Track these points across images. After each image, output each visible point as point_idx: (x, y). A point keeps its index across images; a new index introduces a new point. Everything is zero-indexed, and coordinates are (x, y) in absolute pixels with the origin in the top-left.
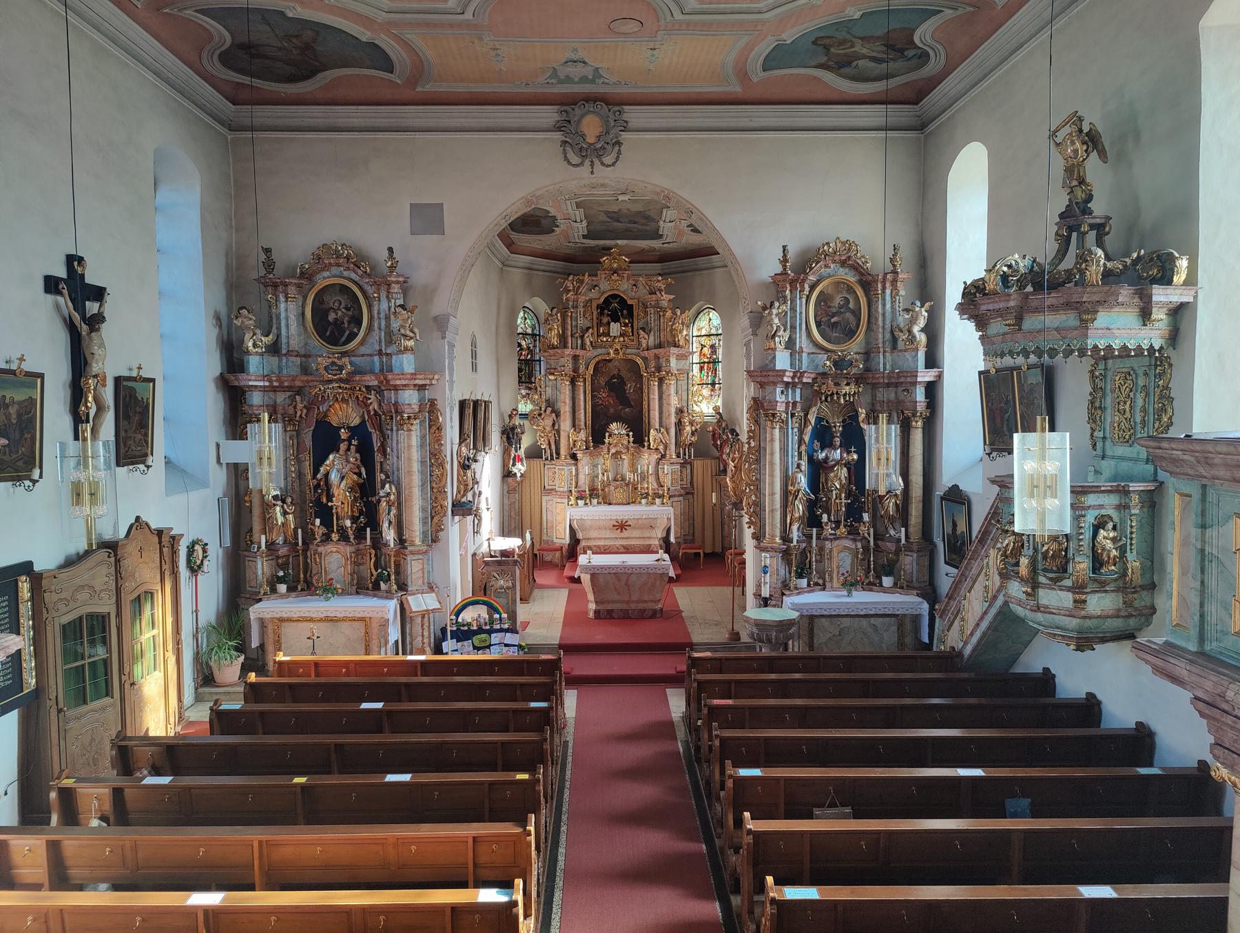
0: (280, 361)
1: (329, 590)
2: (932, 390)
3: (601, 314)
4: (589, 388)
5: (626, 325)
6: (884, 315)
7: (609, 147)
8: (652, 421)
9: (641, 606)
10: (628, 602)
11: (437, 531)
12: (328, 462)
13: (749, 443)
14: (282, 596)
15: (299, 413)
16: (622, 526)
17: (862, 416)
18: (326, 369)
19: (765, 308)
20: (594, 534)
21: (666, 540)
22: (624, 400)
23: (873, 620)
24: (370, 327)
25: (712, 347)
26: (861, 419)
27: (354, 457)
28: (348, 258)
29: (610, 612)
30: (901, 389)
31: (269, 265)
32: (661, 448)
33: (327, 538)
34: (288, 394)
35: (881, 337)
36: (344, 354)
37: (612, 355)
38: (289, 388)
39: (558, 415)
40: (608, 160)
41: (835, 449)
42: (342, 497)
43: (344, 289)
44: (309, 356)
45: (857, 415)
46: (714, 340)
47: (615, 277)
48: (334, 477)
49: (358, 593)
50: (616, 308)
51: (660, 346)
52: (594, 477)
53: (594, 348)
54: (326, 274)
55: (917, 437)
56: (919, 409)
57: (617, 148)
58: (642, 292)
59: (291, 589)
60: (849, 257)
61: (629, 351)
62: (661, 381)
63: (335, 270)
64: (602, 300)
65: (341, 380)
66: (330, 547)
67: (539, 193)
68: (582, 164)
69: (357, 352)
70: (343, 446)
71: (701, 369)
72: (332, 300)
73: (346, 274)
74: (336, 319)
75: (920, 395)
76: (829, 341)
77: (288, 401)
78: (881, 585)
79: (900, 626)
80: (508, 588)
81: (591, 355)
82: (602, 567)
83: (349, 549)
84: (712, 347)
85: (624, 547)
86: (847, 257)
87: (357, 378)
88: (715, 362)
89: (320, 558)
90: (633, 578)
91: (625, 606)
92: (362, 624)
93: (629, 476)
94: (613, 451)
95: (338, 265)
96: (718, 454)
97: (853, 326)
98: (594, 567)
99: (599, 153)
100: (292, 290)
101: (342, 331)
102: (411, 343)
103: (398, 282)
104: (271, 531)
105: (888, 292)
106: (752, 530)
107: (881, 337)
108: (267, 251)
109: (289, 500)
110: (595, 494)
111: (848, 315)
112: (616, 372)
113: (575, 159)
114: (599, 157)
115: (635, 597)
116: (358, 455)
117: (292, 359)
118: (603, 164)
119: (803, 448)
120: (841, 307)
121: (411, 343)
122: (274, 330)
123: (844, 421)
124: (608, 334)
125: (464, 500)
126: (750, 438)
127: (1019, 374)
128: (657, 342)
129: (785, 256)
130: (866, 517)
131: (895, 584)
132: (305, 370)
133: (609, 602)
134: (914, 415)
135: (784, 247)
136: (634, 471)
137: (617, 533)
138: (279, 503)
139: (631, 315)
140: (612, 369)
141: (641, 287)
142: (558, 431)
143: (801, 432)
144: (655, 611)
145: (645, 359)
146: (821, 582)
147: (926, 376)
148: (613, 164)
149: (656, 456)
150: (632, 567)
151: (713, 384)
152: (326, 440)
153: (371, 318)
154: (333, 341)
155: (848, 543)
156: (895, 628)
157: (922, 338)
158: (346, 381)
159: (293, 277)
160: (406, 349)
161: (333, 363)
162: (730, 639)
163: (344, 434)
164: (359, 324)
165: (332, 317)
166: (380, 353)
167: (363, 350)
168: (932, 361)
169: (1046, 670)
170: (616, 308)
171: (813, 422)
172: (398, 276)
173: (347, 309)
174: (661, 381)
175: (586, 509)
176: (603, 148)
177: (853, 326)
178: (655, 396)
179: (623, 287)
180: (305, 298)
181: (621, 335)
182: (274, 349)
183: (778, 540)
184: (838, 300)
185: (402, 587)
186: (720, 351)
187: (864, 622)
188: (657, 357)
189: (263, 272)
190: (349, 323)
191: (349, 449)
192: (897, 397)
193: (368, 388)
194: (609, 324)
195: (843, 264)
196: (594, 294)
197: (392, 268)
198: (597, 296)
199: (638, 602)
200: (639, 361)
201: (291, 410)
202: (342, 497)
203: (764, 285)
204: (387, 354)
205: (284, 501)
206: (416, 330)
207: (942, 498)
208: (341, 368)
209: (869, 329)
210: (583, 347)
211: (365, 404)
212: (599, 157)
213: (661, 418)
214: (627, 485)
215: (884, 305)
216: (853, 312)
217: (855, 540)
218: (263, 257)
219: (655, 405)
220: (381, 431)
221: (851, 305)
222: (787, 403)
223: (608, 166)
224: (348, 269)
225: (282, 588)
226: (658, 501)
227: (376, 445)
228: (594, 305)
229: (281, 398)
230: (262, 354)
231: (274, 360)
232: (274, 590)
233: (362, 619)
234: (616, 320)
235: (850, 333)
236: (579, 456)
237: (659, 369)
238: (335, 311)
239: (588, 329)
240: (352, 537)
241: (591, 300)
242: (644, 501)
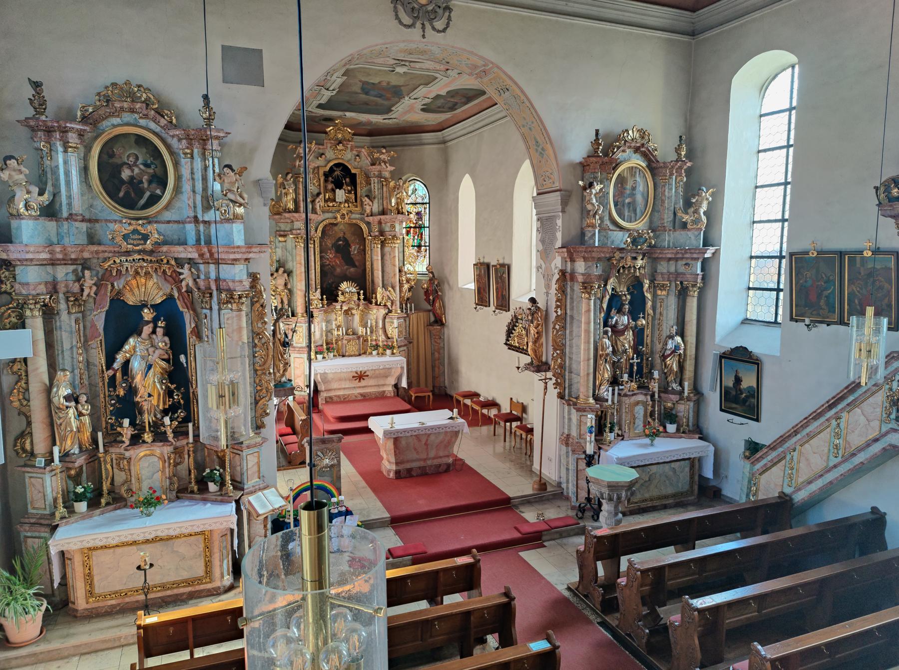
0: (58, 227)
1: (151, 502)
3: (326, 181)
4: (317, 250)
5: (350, 192)
7: (440, 11)
8: (376, 280)
9: (436, 462)
10: (425, 460)
11: (262, 416)
12: (127, 347)
13: (556, 312)
14: (84, 517)
15: (85, 293)
16: (360, 376)
18: (126, 237)
19: (584, 188)
20: (335, 385)
21: (396, 386)
22: (348, 259)
23: (673, 465)
24: (177, 190)
25: (418, 214)
27: (162, 342)
28: (147, 103)
29: (409, 471)
30: (680, 263)
31: (39, 103)
32: (389, 304)
33: (136, 440)
34: (72, 268)
36: (149, 220)
37: (339, 219)
38: (74, 262)
39: (289, 273)
40: (439, 25)
41: (624, 314)
42: (150, 387)
43: (141, 141)
44: (97, 221)
45: (642, 286)
46: (420, 208)
47: (340, 147)
48: (137, 365)
49: (178, 498)
50: (341, 177)
51: (383, 213)
52: (329, 332)
53: (323, 212)
54: (116, 121)
55: (692, 304)
57: (447, 14)
58: (366, 161)
59: (94, 504)
60: (643, 145)
61: (353, 216)
62: (383, 244)
63: (127, 117)
64: (327, 168)
65: (143, 251)
66: (141, 452)
67: (365, 52)
68: (412, 26)
69: (160, 218)
70: (147, 329)
71: (408, 233)
72: (126, 154)
73: (143, 122)
74: (132, 178)
77: (71, 277)
78: (666, 432)
79: (692, 466)
80: (332, 466)
81: (320, 218)
82: (405, 431)
83: (167, 450)
84: (418, 214)
85: (361, 395)
87: (165, 249)
88: (420, 227)
89: (129, 462)
90: (432, 438)
91: (422, 464)
92: (201, 538)
93: (361, 331)
94: (345, 308)
95: (132, 111)
96: (430, 308)
98: (398, 431)
99: (432, 16)
100: (73, 138)
101: (141, 193)
102: (240, 210)
103: (217, 138)
104: (63, 439)
106: (557, 390)
108: (37, 85)
109: (83, 399)
110: (330, 347)
112: (341, 235)
113: (407, 20)
114: (431, 20)
115: (432, 454)
116: (167, 339)
117: (77, 224)
118: (434, 29)
121: (240, 210)
122: (49, 188)
124: (334, 200)
125: (284, 379)
126: (557, 307)
127: (852, 261)
128: (381, 208)
129: (597, 139)
130: (656, 374)
131: (678, 430)
132: (92, 239)
133: (408, 461)
136: (365, 326)
137: (356, 383)
138: (73, 404)
139: (353, 183)
140: (339, 231)
141: (363, 158)
142: (290, 291)
144: (448, 465)
145: (368, 224)
148: (444, 30)
149: (383, 311)
150: (432, 428)
151: (419, 246)
152: (123, 323)
153: (178, 178)
154: (128, 203)
155: (641, 398)
156: (687, 469)
158: (151, 252)
159: (73, 119)
160: (236, 217)
161: (135, 231)
162: (540, 489)
163: (147, 314)
164: (163, 184)
165: (126, 174)
166: (196, 220)
167: (167, 216)
169: (875, 510)
170: (341, 177)
172: (218, 130)
173: (146, 165)
174: (383, 244)
175: (324, 363)
176: (434, 11)
178: (377, 257)
179: (347, 157)
180: (88, 149)
181: (346, 201)
182: (50, 212)
183: (591, 401)
185: (238, 485)
186: (426, 218)
187: (667, 466)
188: (380, 223)
189: (31, 112)
190: (150, 182)
191: (154, 332)
193: (180, 262)
194: (333, 191)
195: (637, 150)
196: (321, 162)
197: (209, 120)
198: (323, 165)
199: (434, 458)
200: (364, 227)
201: (76, 288)
202: (150, 387)
203: (573, 166)
204: (205, 222)
205: (77, 402)
206: (245, 196)
207: (723, 356)
208: (145, 237)
210: (314, 211)
211: (176, 279)
212: (431, 20)
213: (383, 277)
214: (359, 338)
217: (646, 395)
218: (29, 92)
219: (378, 265)
220: (194, 310)
223: (439, 31)
224: (146, 116)
225: (82, 507)
226: (388, 352)
227: (189, 327)
228: (321, 172)
229: (62, 273)
230: (36, 218)
231: (52, 225)
232: (71, 511)
233: (202, 533)
234: (340, 186)
236: (316, 313)
237: (382, 233)
238: (130, 167)
239: (318, 194)
240: (170, 436)
241: (318, 167)
242: (374, 353)
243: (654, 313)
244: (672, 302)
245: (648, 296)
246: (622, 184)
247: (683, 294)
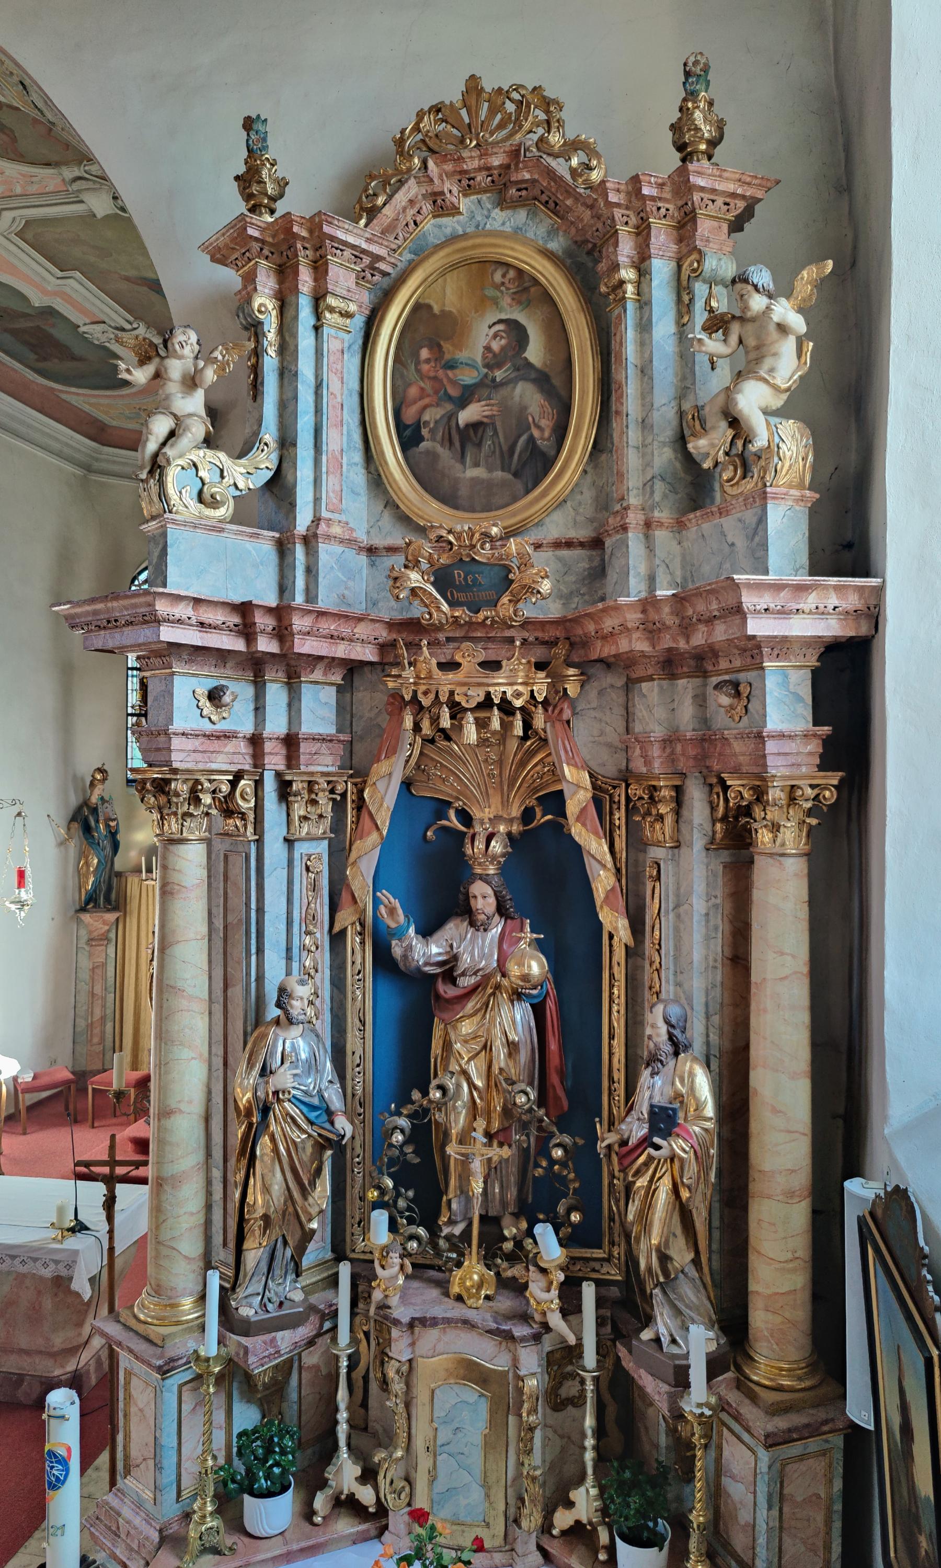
2: (846, 677)
6: (645, 370)
17: (578, 800)
26: (572, 808)
35: (643, 460)
56: (777, 767)
75: (784, 705)
76: (449, 499)
86: (487, 142)
97: (543, 435)
105: (661, 269)
107: (643, 460)
111: (527, 396)
119: (346, 917)
120: (493, 361)
123: (527, 815)
134: (760, 794)
135: (249, 124)
143: (339, 854)
146: (366, 1495)
147: (818, 613)
157: (791, 448)
168: (846, 542)
171: (384, 819)
177: (543, 435)
184: (482, 336)
192: (704, 721)
195: (503, 188)
209: (602, 445)
215: (645, 327)
216: (542, 380)
221: (535, 353)
222: (256, 741)
235: (535, 464)
243: (637, 925)
244: (690, 880)
245: (594, 845)
246: (436, 347)
247: (736, 840)
